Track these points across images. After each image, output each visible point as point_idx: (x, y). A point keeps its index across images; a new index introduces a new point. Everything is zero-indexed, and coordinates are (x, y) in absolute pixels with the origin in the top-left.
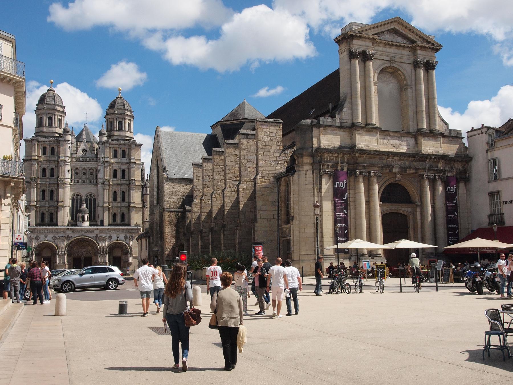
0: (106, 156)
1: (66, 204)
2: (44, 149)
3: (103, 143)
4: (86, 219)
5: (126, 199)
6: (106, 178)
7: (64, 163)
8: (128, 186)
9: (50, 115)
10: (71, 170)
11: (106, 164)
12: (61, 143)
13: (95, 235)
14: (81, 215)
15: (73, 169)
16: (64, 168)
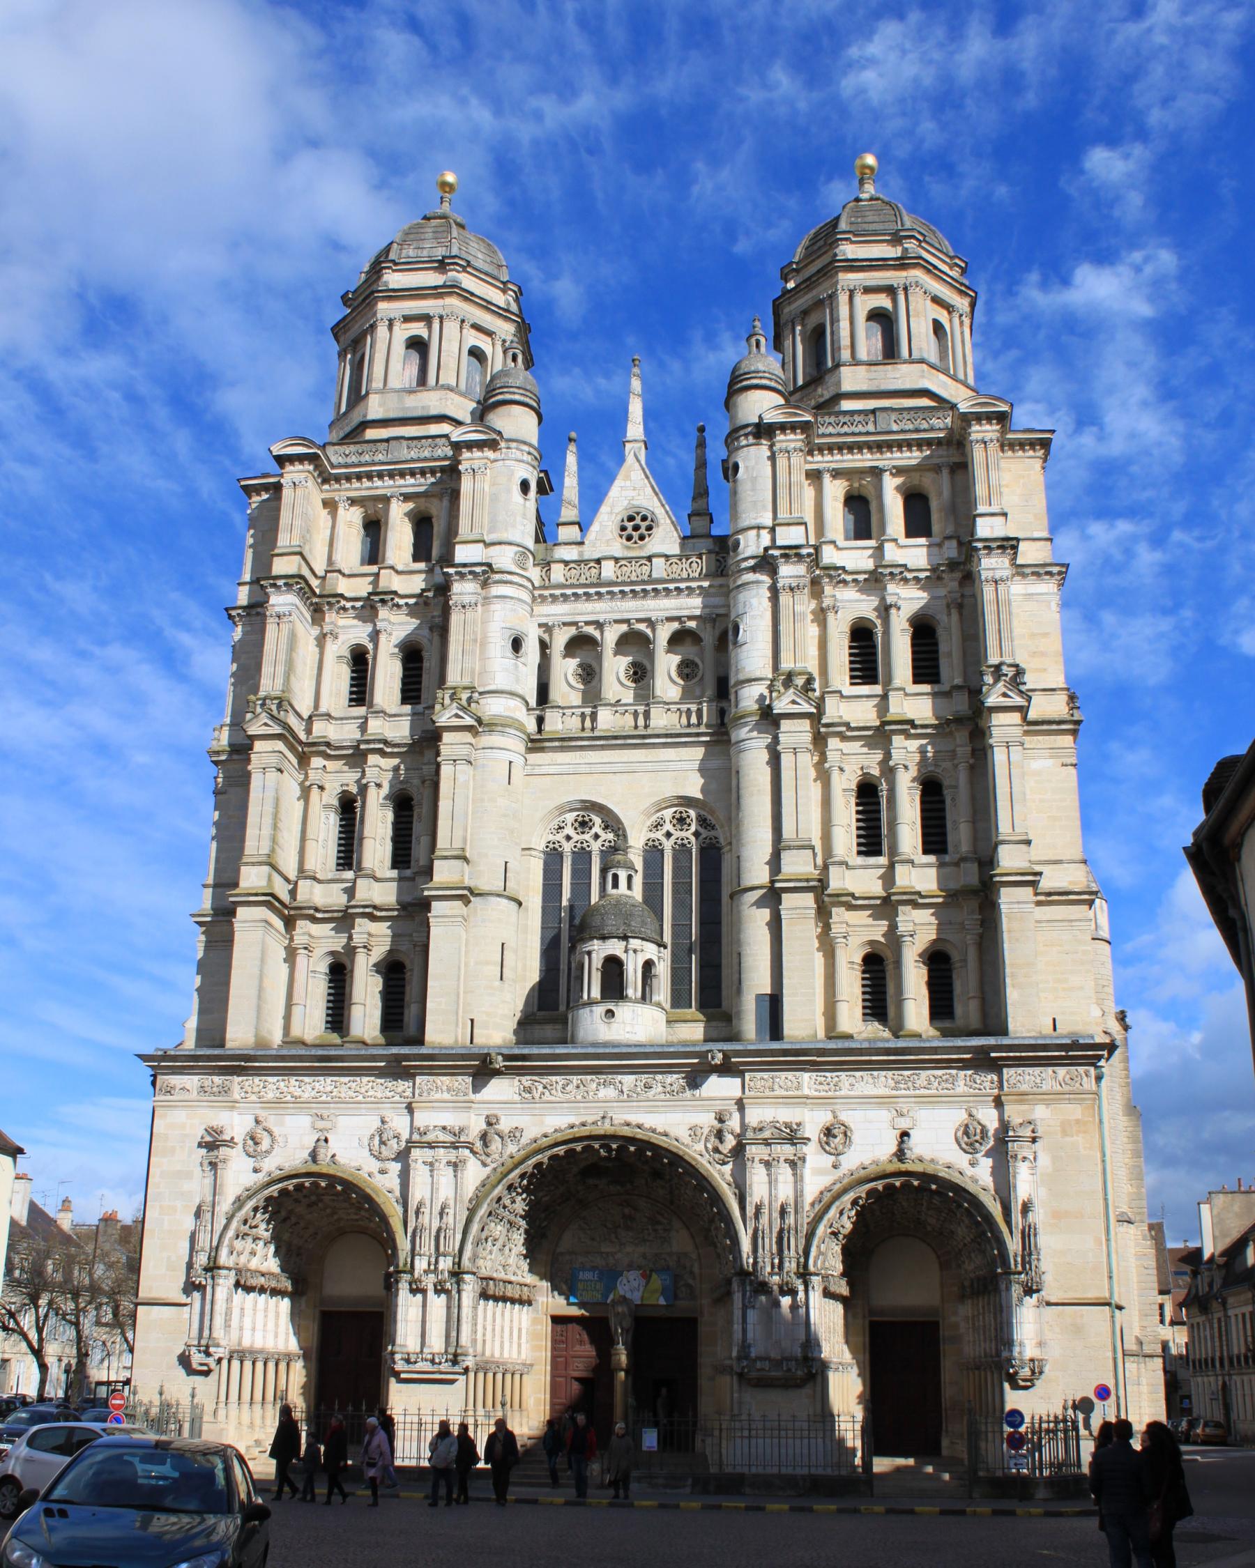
0: (783, 515)
1: (488, 880)
2: (374, 528)
3: (763, 431)
4: (633, 985)
5: (960, 835)
6: (786, 664)
7: (485, 584)
8: (962, 736)
9: (418, 329)
10: (544, 646)
11: (789, 572)
12: (469, 459)
13: (707, 1120)
14: (600, 950)
15: (560, 639)
16: (485, 622)
